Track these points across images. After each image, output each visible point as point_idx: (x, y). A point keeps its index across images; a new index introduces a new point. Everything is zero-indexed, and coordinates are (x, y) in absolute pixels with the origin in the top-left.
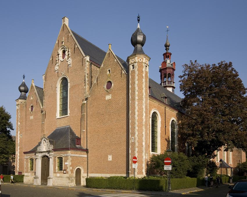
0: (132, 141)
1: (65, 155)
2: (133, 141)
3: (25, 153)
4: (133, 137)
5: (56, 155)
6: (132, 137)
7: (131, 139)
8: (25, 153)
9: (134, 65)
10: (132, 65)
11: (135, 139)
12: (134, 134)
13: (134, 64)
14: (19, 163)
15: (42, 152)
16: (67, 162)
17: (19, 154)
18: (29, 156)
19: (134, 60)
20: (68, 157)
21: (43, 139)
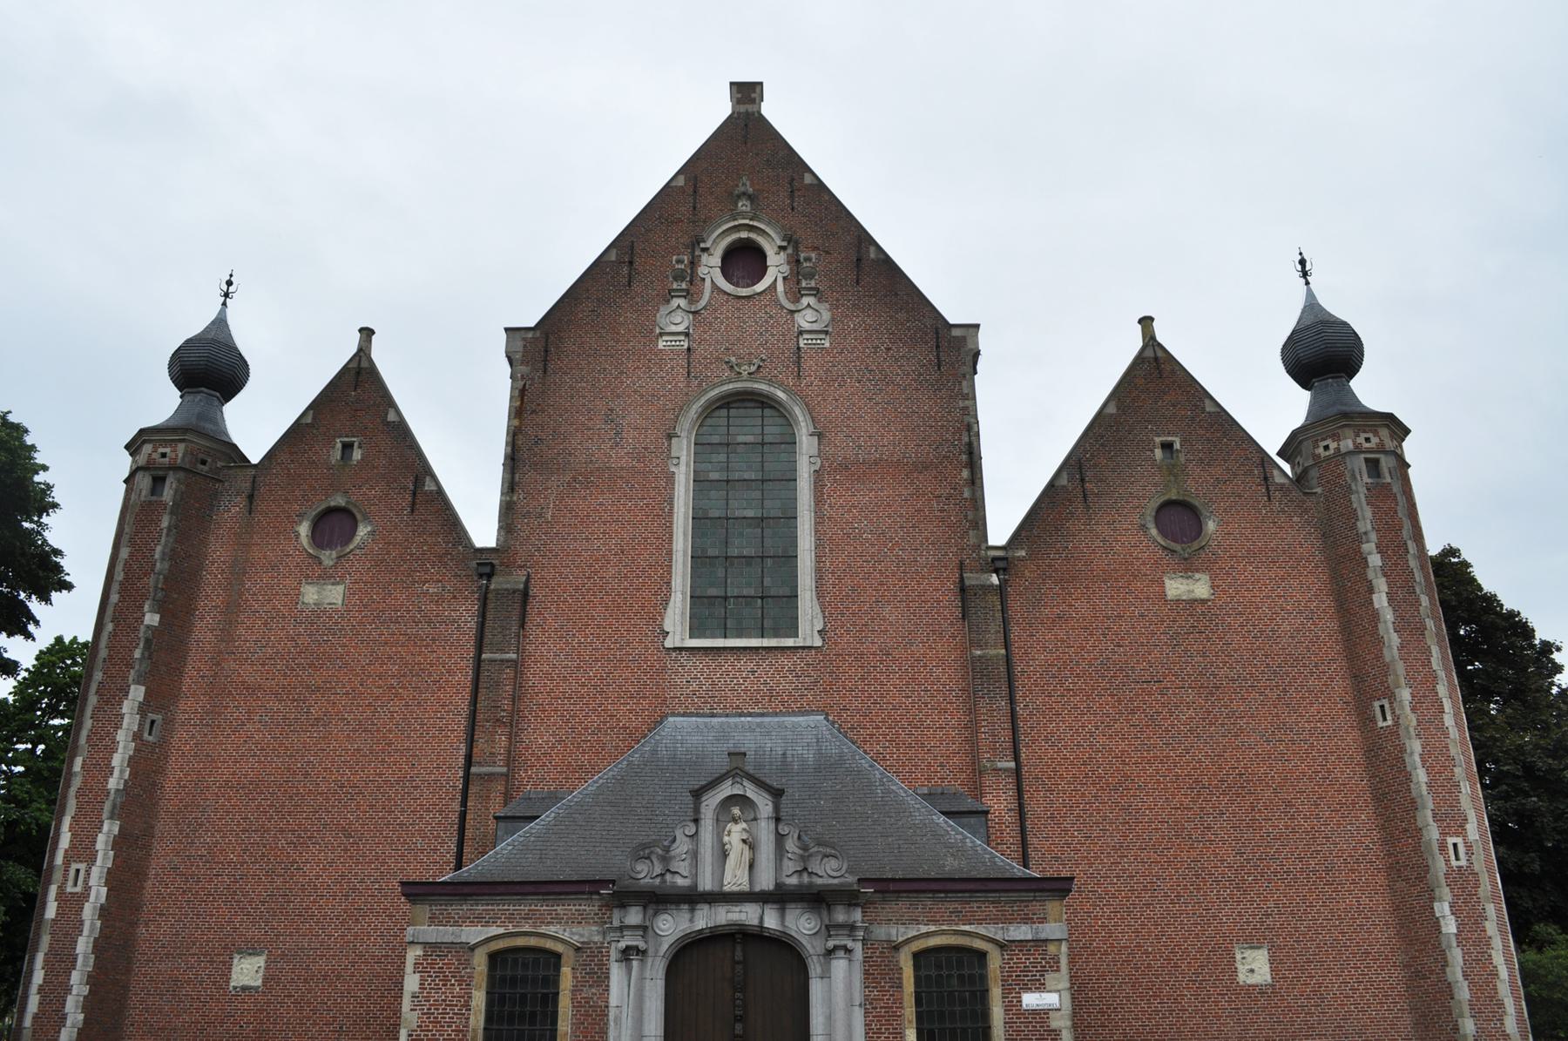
0: (1454, 863)
1: (1021, 932)
2: (1463, 863)
3: (417, 892)
4: (1459, 840)
5: (899, 933)
6: (1451, 840)
7: (1443, 847)
8: (417, 892)
9: (1377, 461)
10: (1367, 460)
11: (1469, 853)
12: (1452, 822)
13: (1382, 457)
14: (92, 980)
15: (693, 898)
16: (1041, 987)
17: (99, 893)
18: (479, 920)
19: (1375, 440)
20: (1052, 948)
21: (726, 790)
